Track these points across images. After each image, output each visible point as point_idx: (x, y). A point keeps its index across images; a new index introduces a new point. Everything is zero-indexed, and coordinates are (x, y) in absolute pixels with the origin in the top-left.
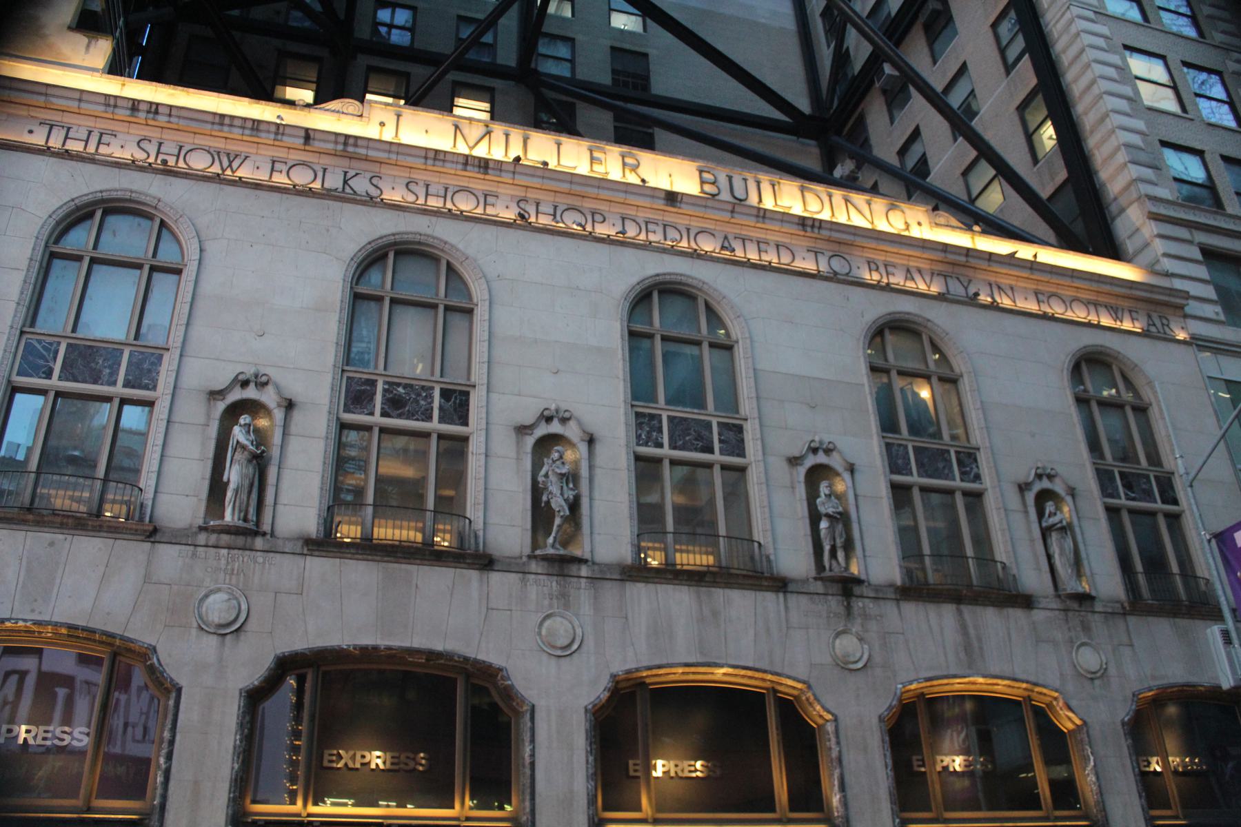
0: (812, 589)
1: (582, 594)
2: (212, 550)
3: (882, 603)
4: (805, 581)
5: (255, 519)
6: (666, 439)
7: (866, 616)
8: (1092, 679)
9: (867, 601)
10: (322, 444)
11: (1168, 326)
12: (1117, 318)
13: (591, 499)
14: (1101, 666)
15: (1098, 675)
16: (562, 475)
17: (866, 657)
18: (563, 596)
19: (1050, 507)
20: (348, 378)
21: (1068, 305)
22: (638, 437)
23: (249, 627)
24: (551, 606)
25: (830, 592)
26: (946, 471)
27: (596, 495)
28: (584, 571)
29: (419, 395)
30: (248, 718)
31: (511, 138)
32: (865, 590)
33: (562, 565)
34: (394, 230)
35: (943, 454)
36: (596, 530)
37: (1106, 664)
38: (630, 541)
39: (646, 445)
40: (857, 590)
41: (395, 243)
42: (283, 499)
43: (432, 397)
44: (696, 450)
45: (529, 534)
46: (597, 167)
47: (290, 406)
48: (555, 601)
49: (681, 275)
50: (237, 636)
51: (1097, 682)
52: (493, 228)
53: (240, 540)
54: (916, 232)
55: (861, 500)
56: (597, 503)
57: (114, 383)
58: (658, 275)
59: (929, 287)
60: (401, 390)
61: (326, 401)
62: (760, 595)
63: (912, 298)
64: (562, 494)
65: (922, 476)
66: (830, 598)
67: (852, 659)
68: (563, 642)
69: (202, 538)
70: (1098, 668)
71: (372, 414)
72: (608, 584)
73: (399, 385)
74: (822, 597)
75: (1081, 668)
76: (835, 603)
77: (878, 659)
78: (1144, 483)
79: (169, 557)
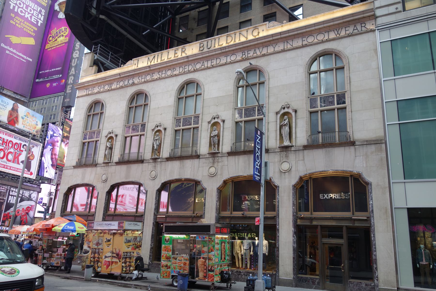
0: (206, 157)
1: (158, 166)
2: (104, 167)
3: (223, 157)
4: (205, 155)
5: (110, 160)
6: (181, 125)
7: (218, 162)
8: (284, 172)
9: (219, 157)
10: (120, 142)
11: (364, 27)
12: (338, 33)
13: (163, 143)
14: (289, 167)
15: (287, 171)
16: (157, 140)
17: (216, 173)
18: (155, 166)
19: (286, 117)
20: (126, 127)
21: (315, 37)
22: (176, 125)
23: (108, 180)
24: (153, 169)
25: (210, 157)
26: (253, 114)
27: (165, 142)
28: (159, 160)
29: (137, 127)
30: (107, 197)
31: (159, 56)
32: (219, 155)
33: (155, 160)
34: (136, 90)
35: (253, 109)
36: (164, 150)
37: (291, 167)
38: (169, 151)
39: (177, 127)
40: (217, 155)
41: (136, 93)
42: (115, 155)
43: (139, 127)
44: (188, 125)
45: (151, 154)
46: (176, 55)
47: (116, 136)
48: (154, 168)
49: (190, 79)
50: (106, 183)
51: (287, 173)
52: (153, 82)
53: (107, 165)
54: (261, 35)
55: (225, 129)
56: (164, 144)
57: (94, 138)
58: (184, 81)
59: (261, 53)
60: (134, 127)
61: (121, 133)
62: (194, 160)
63: (254, 59)
64: (156, 144)
65: (246, 118)
66: (210, 158)
67: (212, 174)
68: (153, 177)
69: (103, 165)
70: (288, 168)
71: (129, 134)
72: (163, 163)
73: (134, 126)
74: (208, 158)
75: (282, 169)
76: (211, 160)
77: (219, 173)
78: (331, 99)
79: (99, 170)
